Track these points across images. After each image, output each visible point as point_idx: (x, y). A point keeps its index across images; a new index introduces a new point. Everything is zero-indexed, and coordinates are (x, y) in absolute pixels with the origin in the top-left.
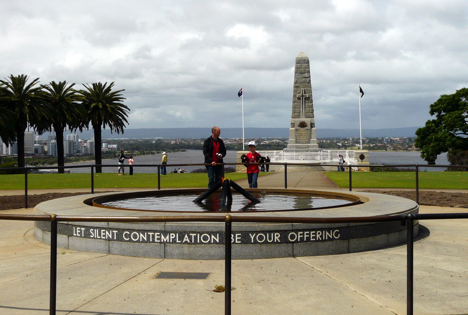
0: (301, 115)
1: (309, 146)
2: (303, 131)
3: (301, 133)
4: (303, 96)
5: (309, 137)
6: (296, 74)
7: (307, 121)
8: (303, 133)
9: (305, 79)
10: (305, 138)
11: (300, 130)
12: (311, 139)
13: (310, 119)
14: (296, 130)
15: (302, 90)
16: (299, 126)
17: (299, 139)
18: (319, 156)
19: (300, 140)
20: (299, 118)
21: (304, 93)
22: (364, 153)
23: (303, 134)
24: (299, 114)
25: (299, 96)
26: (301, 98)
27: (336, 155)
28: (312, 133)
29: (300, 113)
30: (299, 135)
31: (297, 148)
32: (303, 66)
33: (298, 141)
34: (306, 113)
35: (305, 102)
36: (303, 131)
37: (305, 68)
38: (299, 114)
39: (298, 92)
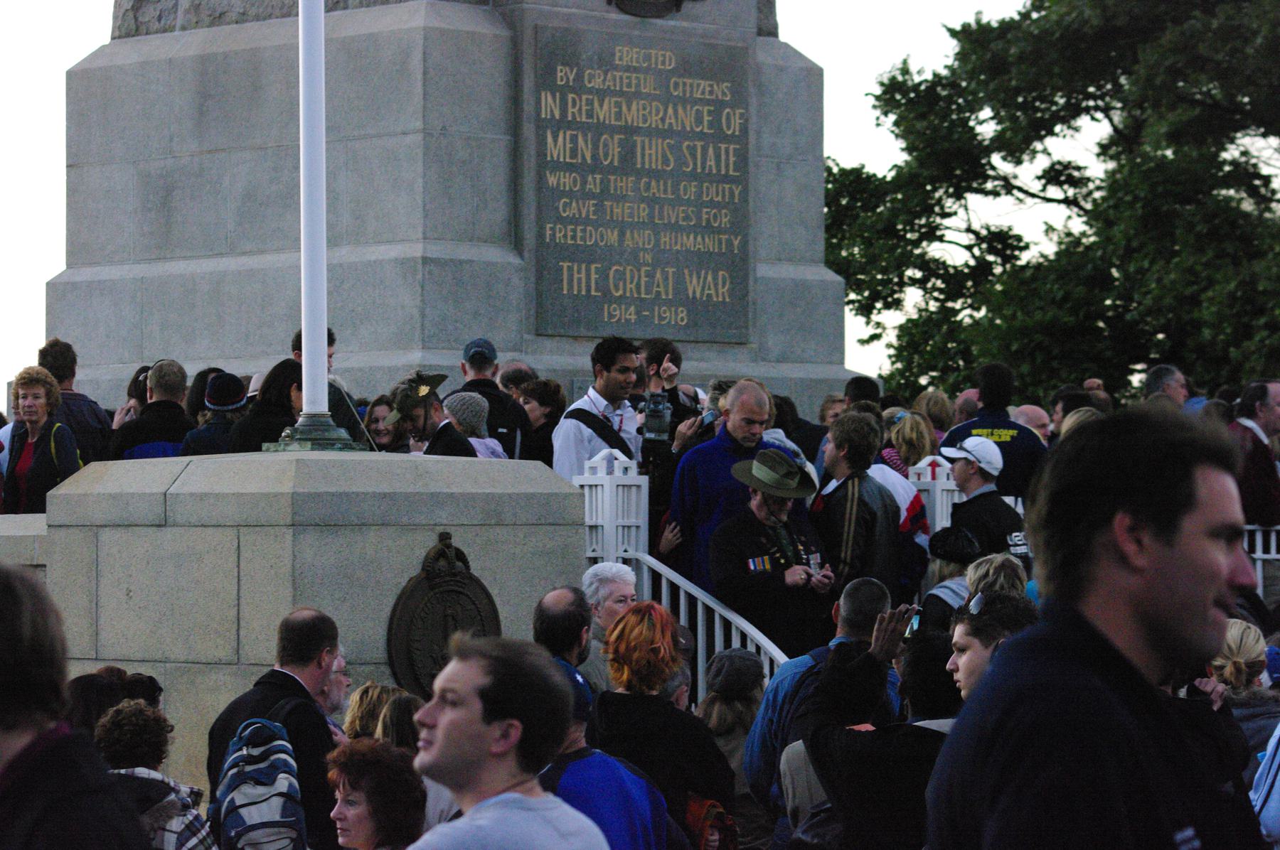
3: (630, 131)
8: (651, 133)
10: (675, 228)
19: (604, 275)
23: (651, 153)
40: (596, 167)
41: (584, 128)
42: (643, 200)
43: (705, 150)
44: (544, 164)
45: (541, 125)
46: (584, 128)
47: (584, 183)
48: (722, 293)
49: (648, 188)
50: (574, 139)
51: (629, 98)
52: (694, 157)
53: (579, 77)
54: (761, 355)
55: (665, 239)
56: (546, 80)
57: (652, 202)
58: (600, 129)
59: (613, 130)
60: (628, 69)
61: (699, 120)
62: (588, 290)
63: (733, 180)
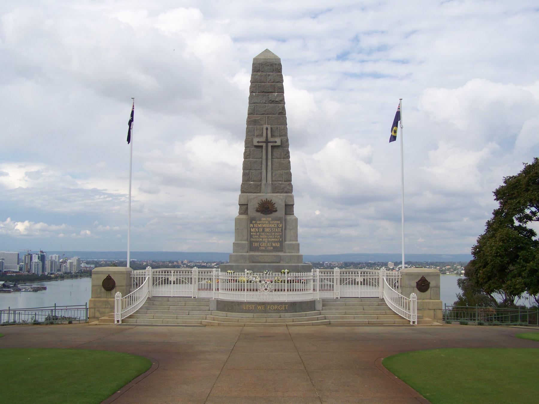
0: (263, 187)
1: (280, 256)
2: (267, 222)
4: (267, 142)
5: (281, 238)
6: (254, 94)
7: (278, 199)
8: (267, 228)
9: (273, 105)
10: (271, 238)
11: (260, 220)
12: (285, 241)
13: (285, 194)
14: (252, 220)
15: (267, 129)
16: (257, 211)
17: (257, 242)
18: (312, 281)
20: (259, 193)
21: (269, 135)
22: (428, 274)
24: (259, 183)
25: (258, 142)
26: (264, 148)
27: (355, 279)
28: (288, 227)
29: (261, 181)
30: (257, 232)
31: (253, 262)
32: (270, 77)
33: (256, 244)
34: (274, 181)
35: (272, 155)
36: (267, 222)
37: (272, 80)
38: (259, 183)
39: (256, 133)
40: (258, 232)
41: (257, 228)
42: (266, 235)
43: (276, 229)
44: (251, 232)
45: (250, 228)
46: (257, 228)
47: (257, 234)
48: (279, 245)
49: (266, 234)
50: (255, 229)
51: (264, 224)
52: (274, 230)
53: (256, 222)
54: (285, 252)
55: (269, 239)
56: (251, 223)
57: (267, 235)
58: (259, 228)
59: (261, 228)
60: (264, 221)
61: (275, 225)
62: (257, 245)
63: (280, 232)
